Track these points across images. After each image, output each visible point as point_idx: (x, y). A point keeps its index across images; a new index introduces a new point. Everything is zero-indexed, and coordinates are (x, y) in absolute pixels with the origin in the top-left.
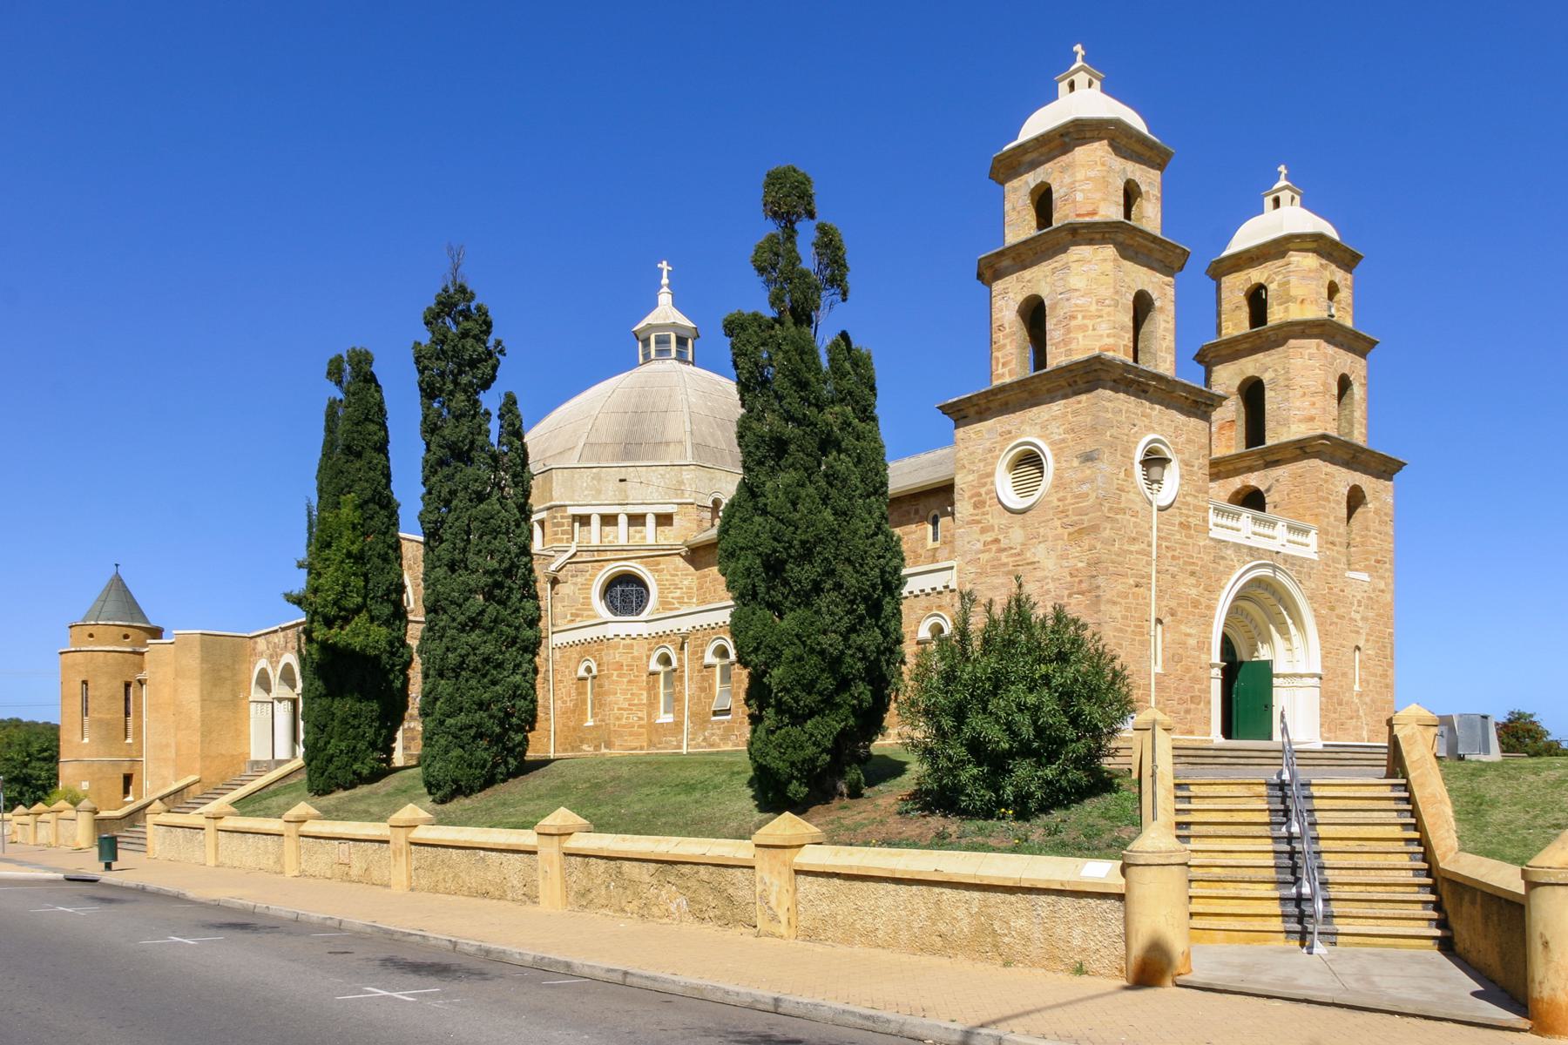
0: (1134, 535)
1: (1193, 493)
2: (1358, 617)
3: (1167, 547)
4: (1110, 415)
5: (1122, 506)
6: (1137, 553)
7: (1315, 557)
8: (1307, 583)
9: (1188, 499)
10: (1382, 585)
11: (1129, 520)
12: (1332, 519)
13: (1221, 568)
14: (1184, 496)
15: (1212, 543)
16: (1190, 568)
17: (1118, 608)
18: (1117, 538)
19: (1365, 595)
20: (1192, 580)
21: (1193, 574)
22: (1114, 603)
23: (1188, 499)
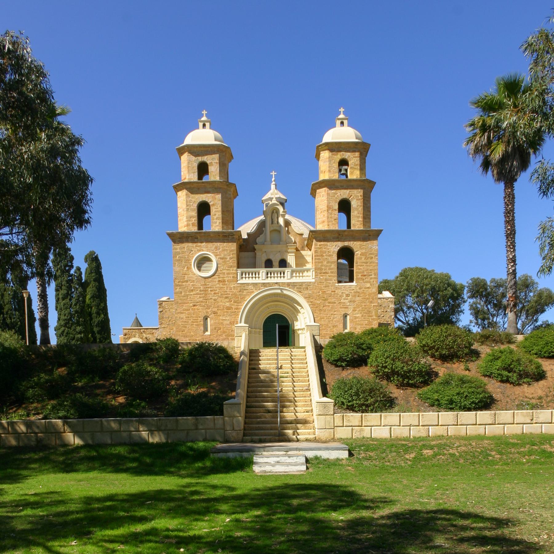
0: (192, 288)
1: (227, 268)
6: (194, 294)
8: (306, 292)
9: (224, 271)
10: (368, 285)
11: (189, 284)
12: (325, 263)
15: (239, 285)
16: (224, 296)
17: (184, 314)
19: (353, 291)
21: (226, 298)
23: (224, 271)
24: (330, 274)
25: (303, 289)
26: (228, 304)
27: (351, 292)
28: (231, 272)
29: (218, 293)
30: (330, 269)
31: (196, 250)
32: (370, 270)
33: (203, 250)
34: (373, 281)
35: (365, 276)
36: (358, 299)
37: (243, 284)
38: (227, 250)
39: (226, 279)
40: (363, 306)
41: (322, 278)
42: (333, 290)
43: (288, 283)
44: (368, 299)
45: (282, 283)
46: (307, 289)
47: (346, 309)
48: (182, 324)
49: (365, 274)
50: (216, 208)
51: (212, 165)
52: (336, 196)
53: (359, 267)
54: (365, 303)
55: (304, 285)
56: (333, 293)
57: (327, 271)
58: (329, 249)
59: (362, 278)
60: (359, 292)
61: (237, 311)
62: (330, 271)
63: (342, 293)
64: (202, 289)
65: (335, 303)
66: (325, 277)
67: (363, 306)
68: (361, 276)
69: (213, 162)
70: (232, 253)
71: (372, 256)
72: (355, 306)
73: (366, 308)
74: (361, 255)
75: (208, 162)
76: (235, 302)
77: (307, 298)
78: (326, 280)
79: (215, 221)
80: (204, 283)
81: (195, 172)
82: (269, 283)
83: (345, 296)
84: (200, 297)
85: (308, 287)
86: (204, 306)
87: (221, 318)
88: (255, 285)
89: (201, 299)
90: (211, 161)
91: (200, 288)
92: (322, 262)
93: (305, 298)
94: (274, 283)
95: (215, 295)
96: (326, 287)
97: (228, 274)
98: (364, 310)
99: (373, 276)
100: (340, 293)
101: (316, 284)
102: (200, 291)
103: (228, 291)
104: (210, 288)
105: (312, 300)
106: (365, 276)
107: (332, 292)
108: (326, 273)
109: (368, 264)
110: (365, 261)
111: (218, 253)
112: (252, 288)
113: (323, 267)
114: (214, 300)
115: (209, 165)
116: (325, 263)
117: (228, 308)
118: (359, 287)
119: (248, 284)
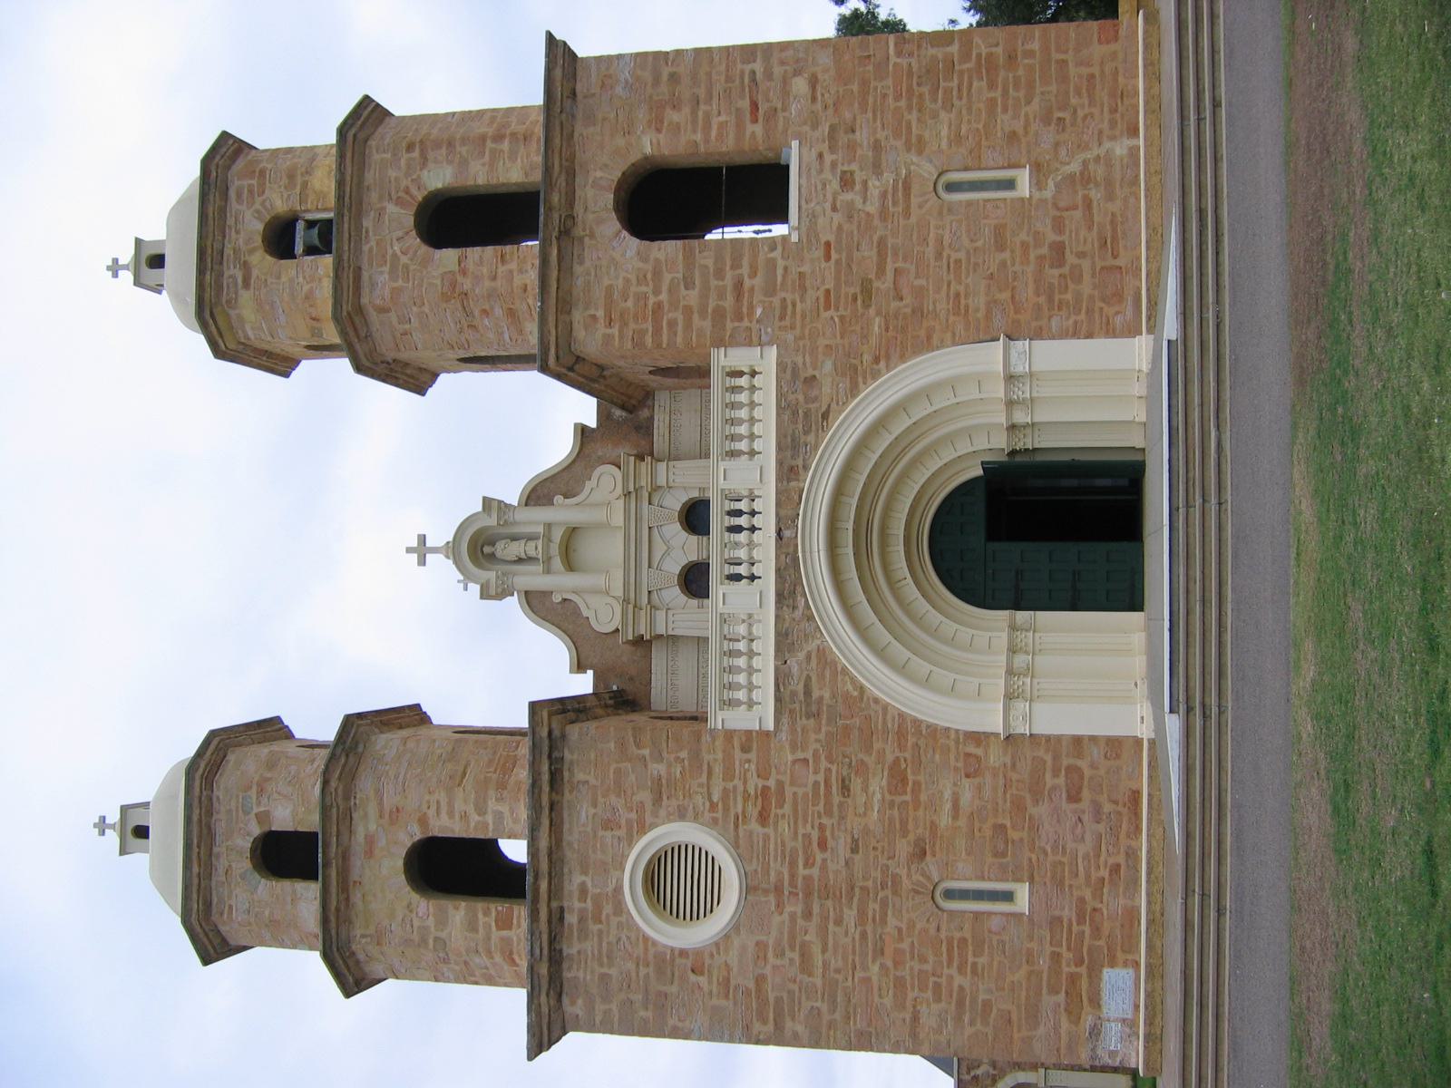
0: (796, 956)
2: (875, 186)
3: (806, 865)
4: (614, 1007)
5: (752, 985)
6: (824, 951)
7: (772, 352)
10: (800, 85)
11: (775, 967)
12: (692, 297)
13: (827, 695)
14: (713, 807)
15: (785, 720)
16: (836, 799)
17: (923, 1009)
18: (807, 1005)
19: (828, 158)
20: (856, 785)
21: (845, 789)
22: (915, 1018)
24: (745, 270)
25: (815, 399)
26: (878, 784)
27: (834, 165)
28: (720, 755)
29: (822, 828)
30: (720, 274)
31: (614, 921)
32: (729, 79)
33: (618, 889)
34: (782, 63)
35: (755, 106)
36: (862, 136)
37: (778, 699)
38: (618, 771)
39: (754, 783)
40: (903, 103)
41: (759, 311)
42: (820, 253)
43: (779, 479)
44: (864, 83)
45: (778, 504)
46: (811, 380)
47: (915, 190)
48: (972, 1023)
50: (438, 812)
51: (267, 813)
52: (404, 259)
53: (714, 133)
54: (885, 96)
55: (791, 397)
56: (834, 256)
57: (729, 281)
58: (627, 281)
59: (767, 120)
60: (833, 129)
61: (911, 740)
62: (729, 274)
63: (834, 209)
64: (799, 909)
65: (882, 243)
66: (758, 297)
67: (903, 103)
68: (755, 121)
69: (255, 810)
70: (633, 749)
71: (665, 77)
72: (899, 144)
73: (910, 91)
74: (659, 130)
75: (256, 831)
76: (868, 748)
77: (855, 377)
78: (770, 290)
79: (490, 818)
80: (772, 898)
81: (294, 892)
82: (778, 570)
83: (848, 196)
84: (838, 922)
85: (803, 375)
86: (884, 904)
87: (944, 820)
88: (785, 642)
89: (850, 915)
90: (252, 815)
91: (793, 916)
92: (688, 311)
93: (854, 391)
94: (778, 548)
95: (830, 843)
96: (803, 289)
97: (728, 774)
98: (921, 96)
100: (838, 218)
101: (790, 337)
102: (808, 915)
103: (812, 778)
104: (793, 864)
105: (867, 358)
106: (755, 106)
107: (828, 257)
108: (739, 285)
109: (702, 92)
110: (686, 110)
111: (633, 816)
112: (801, 655)
113: (712, 304)
114: (855, 850)
115: (266, 829)
116: (692, 297)
117: (898, 778)
118: (806, 128)
119: (781, 679)
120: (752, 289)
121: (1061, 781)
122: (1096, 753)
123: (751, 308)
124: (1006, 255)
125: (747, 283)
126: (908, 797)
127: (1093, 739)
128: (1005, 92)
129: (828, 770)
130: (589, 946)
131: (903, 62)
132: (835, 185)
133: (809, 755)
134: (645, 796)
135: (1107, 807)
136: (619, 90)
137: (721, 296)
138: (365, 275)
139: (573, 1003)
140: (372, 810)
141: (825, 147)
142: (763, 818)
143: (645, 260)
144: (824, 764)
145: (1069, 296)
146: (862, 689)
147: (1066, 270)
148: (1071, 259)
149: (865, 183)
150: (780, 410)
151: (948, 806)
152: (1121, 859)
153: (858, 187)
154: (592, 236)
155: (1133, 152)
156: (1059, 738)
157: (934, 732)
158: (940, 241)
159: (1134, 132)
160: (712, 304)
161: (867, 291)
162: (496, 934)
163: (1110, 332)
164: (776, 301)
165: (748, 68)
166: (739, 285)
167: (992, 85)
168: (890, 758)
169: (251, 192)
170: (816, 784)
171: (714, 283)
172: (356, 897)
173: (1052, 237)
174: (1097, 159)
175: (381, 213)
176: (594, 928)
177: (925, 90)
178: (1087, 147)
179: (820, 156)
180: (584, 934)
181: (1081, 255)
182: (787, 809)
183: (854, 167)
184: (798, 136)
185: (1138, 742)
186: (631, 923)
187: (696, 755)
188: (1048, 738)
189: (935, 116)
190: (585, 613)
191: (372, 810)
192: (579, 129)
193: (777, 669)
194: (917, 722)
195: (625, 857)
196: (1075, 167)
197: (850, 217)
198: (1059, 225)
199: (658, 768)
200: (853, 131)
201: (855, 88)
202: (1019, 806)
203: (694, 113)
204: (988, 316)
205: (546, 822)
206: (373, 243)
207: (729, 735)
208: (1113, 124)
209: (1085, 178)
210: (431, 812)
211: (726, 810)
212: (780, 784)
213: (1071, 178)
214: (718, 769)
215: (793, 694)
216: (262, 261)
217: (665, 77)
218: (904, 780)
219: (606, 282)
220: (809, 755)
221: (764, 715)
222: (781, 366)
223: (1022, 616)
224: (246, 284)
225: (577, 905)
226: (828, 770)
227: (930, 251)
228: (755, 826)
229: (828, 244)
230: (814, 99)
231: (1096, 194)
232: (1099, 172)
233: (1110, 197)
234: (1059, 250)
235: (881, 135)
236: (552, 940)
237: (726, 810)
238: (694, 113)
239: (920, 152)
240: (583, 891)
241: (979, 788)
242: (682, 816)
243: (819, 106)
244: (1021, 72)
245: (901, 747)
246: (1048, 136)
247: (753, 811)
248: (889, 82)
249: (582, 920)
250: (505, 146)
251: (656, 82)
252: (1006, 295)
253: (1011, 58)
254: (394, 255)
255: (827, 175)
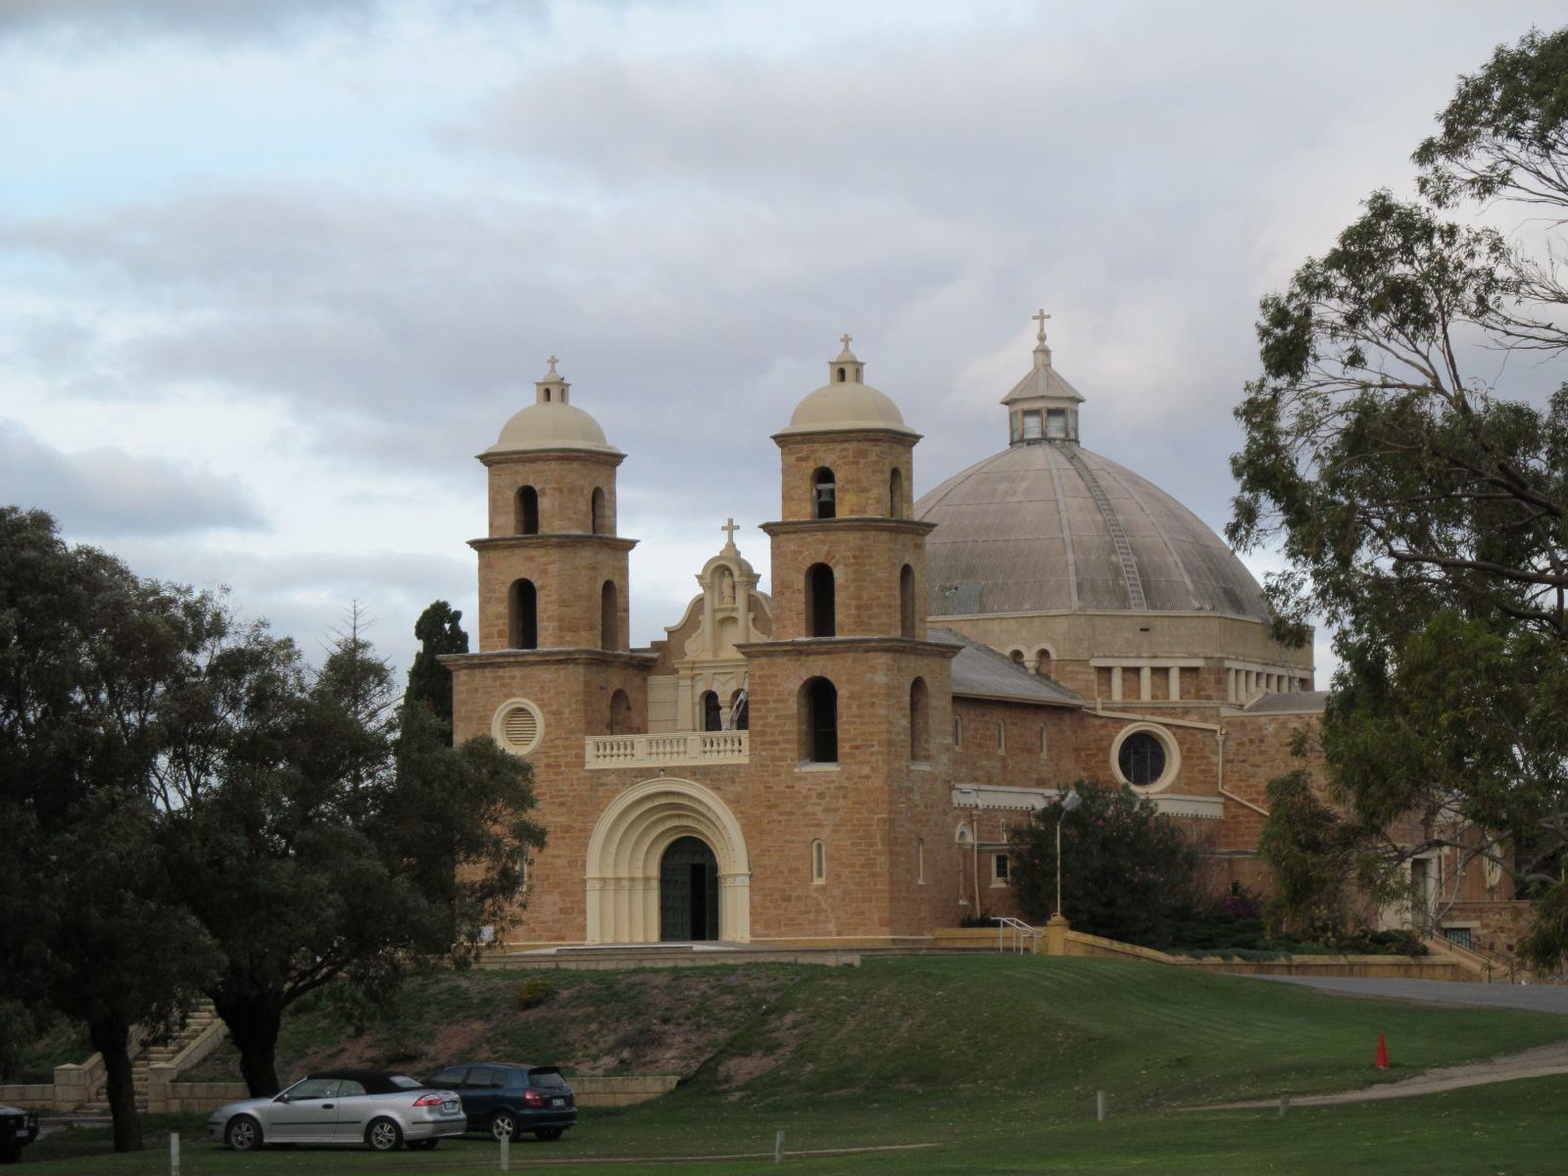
1: (563, 735)
2: (818, 810)
7: (746, 761)
8: (730, 788)
9: (557, 742)
10: (866, 770)
12: (771, 720)
13: (601, 794)
14: (552, 741)
16: (557, 800)
19: (832, 786)
20: (563, 810)
21: (562, 804)
23: (557, 742)
24: (783, 746)
30: (781, 733)
32: (871, 733)
33: (515, 695)
35: (857, 747)
36: (842, 803)
39: (562, 761)
40: (855, 822)
42: (790, 784)
43: (691, 767)
49: (859, 742)
52: (800, 558)
57: (780, 738)
60: (846, 788)
67: (855, 822)
68: (851, 748)
71: (874, 700)
76: (580, 814)
77: (734, 803)
78: (774, 759)
83: (814, 795)
88: (621, 773)
92: (765, 718)
93: (729, 802)
96: (773, 776)
99: (876, 748)
100: (805, 791)
103: (565, 788)
105: (743, 808)
106: (857, 747)
107: (787, 787)
108: (776, 743)
110: (857, 712)
113: (768, 730)
117: (568, 829)
118: (846, 774)
120: (773, 749)
121: (568, 905)
122: (579, 920)
123: (764, 750)
124: (786, 874)
125: (777, 747)
126: (559, 834)
127: (585, 919)
128: (858, 872)
129: (568, 796)
130: (489, 682)
131: (875, 822)
132: (819, 789)
133: (575, 787)
134: (554, 708)
135: (558, 926)
136: (869, 675)
137: (772, 734)
138: (793, 536)
139: (466, 675)
140: (545, 559)
141: (837, 784)
142: (548, 766)
143: (789, 694)
144: (572, 794)
145: (768, 904)
146: (602, 811)
147: (780, 902)
148: (784, 904)
149: (820, 804)
150: (720, 766)
151: (556, 853)
152: (538, 933)
153: (818, 801)
154: (801, 665)
155: (830, 934)
156: (585, 903)
157: (586, 845)
158: (793, 842)
159: (839, 933)
160: (768, 730)
161: (771, 807)
162: (496, 629)
163: (753, 923)
164: (768, 762)
165: (876, 743)
166: (776, 743)
167: (862, 866)
168: (575, 825)
169: (846, 457)
170: (563, 791)
171: (779, 730)
172: (506, 553)
173: (794, 895)
174: (827, 917)
175: (823, 542)
176: (498, 683)
177: (861, 833)
178: (833, 910)
179: (833, 782)
180: (495, 679)
181: (786, 910)
182: (553, 777)
183: (828, 799)
184: (843, 771)
185: (585, 939)
186: (500, 703)
187: (572, 732)
188: (585, 898)
189: (849, 838)
190: (694, 635)
191: (545, 559)
192: (851, 655)
193: (609, 770)
194: (590, 837)
195: (528, 698)
196: (824, 906)
197: (805, 798)
198: (798, 898)
199: (567, 712)
200: (844, 798)
201: (864, 798)
202: (557, 885)
203: (855, 716)
204: (761, 866)
205: (538, 659)
206: (809, 539)
207: (583, 747)
208: (843, 924)
209: (819, 911)
210: (547, 592)
211: (551, 748)
212: (561, 773)
213: (819, 904)
214: (568, 742)
215: (600, 778)
216: (809, 468)
217: (874, 700)
218: (566, 832)
219: (779, 674)
220: (575, 787)
221: (593, 763)
222: (739, 766)
223: (655, 884)
224: (800, 459)
225: (507, 675)
226: (568, 796)
227: (789, 837)
228: (545, 761)
229: (793, 787)
230: (859, 777)
231: (812, 916)
232: (822, 917)
233: (811, 923)
234: (787, 899)
235: (842, 811)
236: (490, 664)
237: (551, 748)
238: (855, 716)
239: (833, 831)
240: (513, 678)
241: (564, 867)
242: (548, 725)
243: (856, 780)
244: (867, 880)
245: (580, 831)
246: (836, 892)
247: (551, 760)
248: (866, 815)
249: (501, 678)
250: (853, 612)
251: (873, 695)
252: (768, 873)
253: (874, 875)
254: (802, 552)
255: (824, 785)
